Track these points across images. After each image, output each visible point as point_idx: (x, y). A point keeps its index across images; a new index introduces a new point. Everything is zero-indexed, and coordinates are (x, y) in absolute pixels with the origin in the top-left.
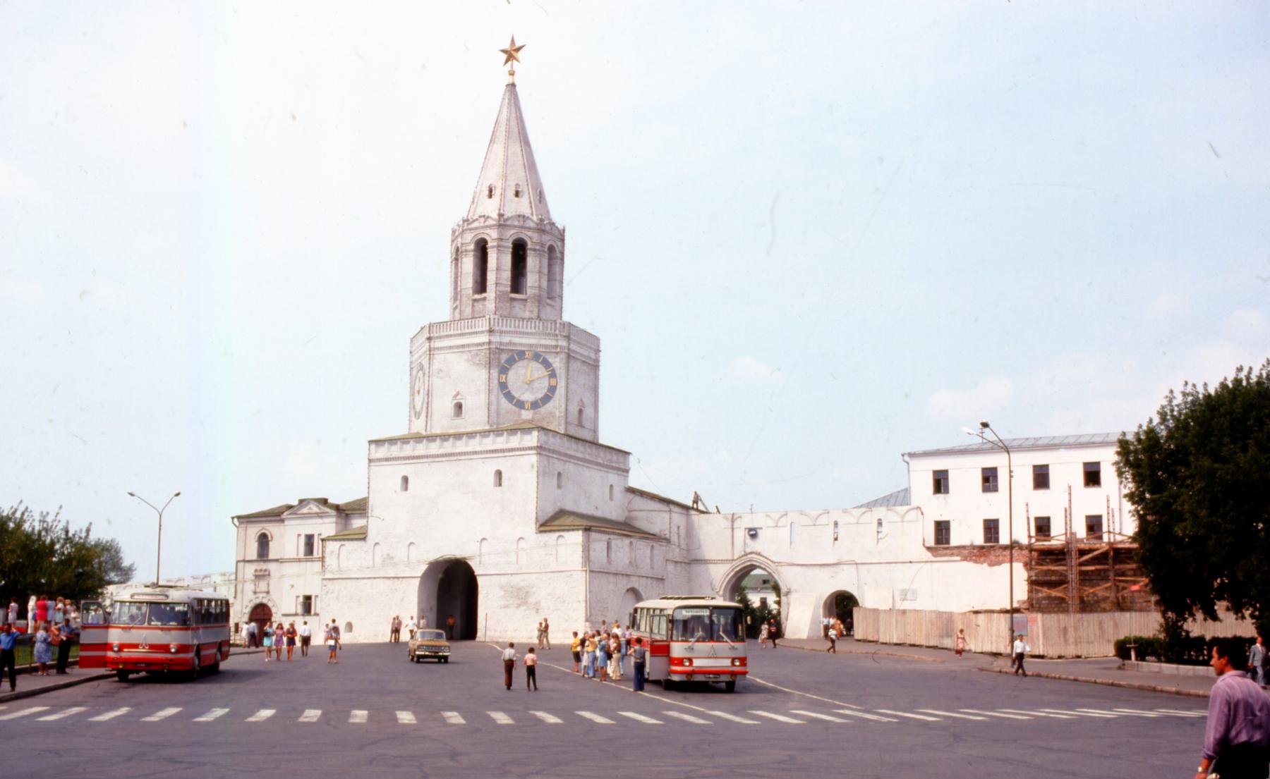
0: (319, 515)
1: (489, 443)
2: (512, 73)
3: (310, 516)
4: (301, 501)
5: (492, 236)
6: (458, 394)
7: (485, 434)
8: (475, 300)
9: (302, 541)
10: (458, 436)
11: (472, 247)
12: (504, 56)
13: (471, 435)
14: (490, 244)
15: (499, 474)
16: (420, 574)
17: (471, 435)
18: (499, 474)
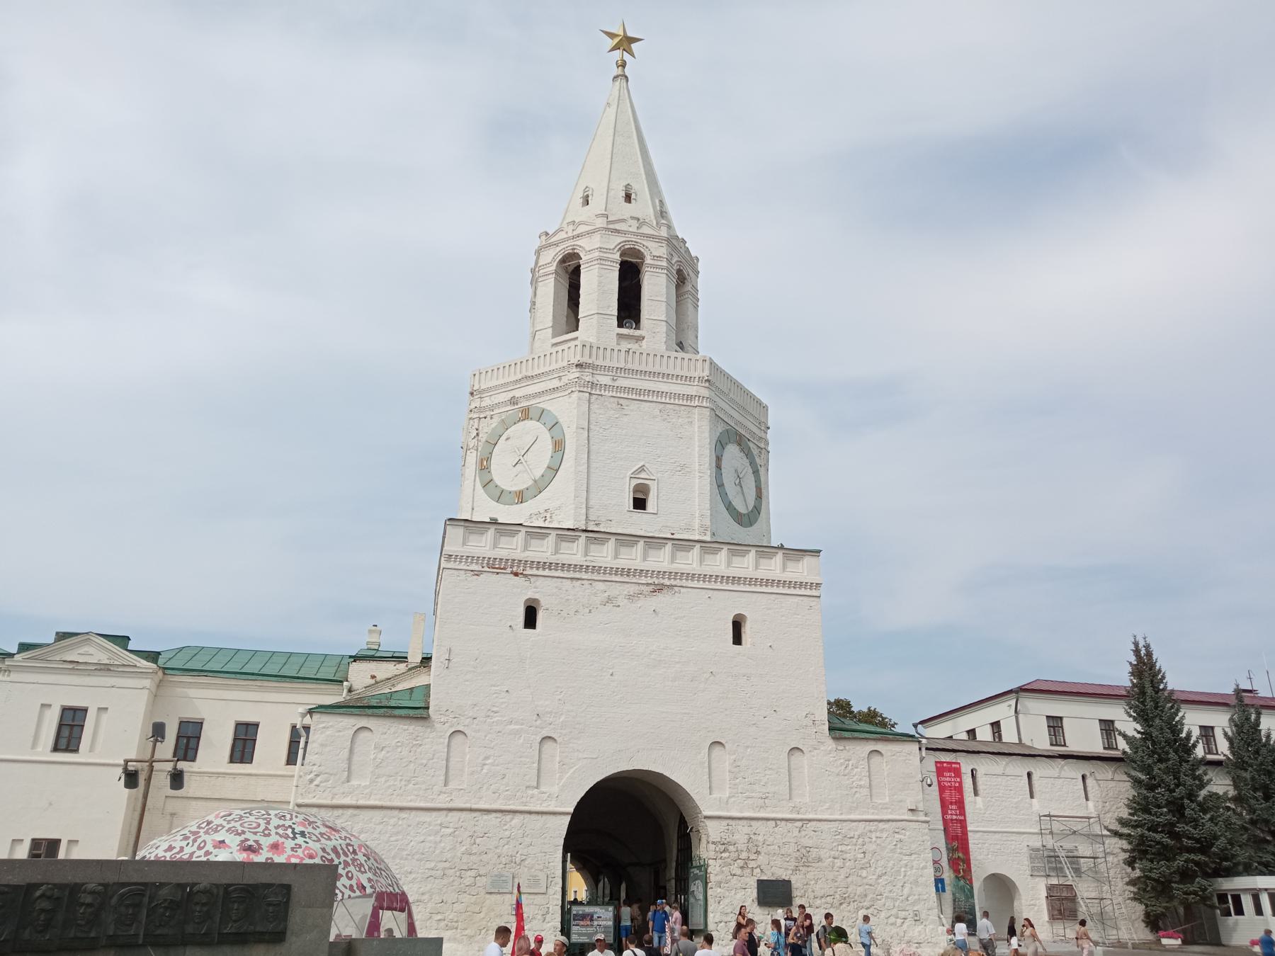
0: (105, 669)
1: (719, 563)
2: (623, 65)
3: (75, 667)
4: (62, 636)
5: (654, 253)
6: (642, 469)
7: (709, 547)
8: (620, 336)
9: (51, 721)
10: (653, 542)
11: (617, 257)
12: (611, 43)
13: (682, 545)
14: (648, 260)
15: (737, 626)
16: (571, 810)
17: (682, 545)
18: (737, 626)
